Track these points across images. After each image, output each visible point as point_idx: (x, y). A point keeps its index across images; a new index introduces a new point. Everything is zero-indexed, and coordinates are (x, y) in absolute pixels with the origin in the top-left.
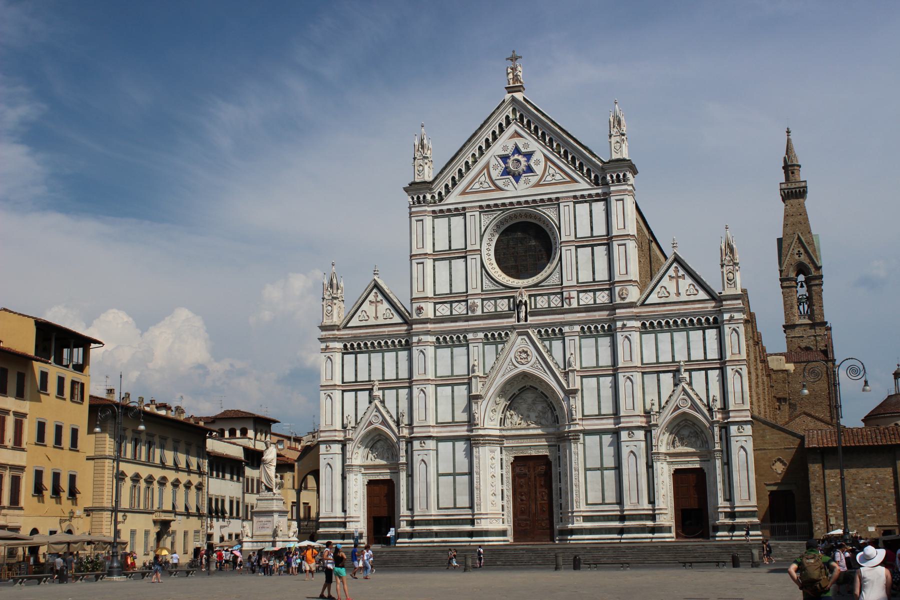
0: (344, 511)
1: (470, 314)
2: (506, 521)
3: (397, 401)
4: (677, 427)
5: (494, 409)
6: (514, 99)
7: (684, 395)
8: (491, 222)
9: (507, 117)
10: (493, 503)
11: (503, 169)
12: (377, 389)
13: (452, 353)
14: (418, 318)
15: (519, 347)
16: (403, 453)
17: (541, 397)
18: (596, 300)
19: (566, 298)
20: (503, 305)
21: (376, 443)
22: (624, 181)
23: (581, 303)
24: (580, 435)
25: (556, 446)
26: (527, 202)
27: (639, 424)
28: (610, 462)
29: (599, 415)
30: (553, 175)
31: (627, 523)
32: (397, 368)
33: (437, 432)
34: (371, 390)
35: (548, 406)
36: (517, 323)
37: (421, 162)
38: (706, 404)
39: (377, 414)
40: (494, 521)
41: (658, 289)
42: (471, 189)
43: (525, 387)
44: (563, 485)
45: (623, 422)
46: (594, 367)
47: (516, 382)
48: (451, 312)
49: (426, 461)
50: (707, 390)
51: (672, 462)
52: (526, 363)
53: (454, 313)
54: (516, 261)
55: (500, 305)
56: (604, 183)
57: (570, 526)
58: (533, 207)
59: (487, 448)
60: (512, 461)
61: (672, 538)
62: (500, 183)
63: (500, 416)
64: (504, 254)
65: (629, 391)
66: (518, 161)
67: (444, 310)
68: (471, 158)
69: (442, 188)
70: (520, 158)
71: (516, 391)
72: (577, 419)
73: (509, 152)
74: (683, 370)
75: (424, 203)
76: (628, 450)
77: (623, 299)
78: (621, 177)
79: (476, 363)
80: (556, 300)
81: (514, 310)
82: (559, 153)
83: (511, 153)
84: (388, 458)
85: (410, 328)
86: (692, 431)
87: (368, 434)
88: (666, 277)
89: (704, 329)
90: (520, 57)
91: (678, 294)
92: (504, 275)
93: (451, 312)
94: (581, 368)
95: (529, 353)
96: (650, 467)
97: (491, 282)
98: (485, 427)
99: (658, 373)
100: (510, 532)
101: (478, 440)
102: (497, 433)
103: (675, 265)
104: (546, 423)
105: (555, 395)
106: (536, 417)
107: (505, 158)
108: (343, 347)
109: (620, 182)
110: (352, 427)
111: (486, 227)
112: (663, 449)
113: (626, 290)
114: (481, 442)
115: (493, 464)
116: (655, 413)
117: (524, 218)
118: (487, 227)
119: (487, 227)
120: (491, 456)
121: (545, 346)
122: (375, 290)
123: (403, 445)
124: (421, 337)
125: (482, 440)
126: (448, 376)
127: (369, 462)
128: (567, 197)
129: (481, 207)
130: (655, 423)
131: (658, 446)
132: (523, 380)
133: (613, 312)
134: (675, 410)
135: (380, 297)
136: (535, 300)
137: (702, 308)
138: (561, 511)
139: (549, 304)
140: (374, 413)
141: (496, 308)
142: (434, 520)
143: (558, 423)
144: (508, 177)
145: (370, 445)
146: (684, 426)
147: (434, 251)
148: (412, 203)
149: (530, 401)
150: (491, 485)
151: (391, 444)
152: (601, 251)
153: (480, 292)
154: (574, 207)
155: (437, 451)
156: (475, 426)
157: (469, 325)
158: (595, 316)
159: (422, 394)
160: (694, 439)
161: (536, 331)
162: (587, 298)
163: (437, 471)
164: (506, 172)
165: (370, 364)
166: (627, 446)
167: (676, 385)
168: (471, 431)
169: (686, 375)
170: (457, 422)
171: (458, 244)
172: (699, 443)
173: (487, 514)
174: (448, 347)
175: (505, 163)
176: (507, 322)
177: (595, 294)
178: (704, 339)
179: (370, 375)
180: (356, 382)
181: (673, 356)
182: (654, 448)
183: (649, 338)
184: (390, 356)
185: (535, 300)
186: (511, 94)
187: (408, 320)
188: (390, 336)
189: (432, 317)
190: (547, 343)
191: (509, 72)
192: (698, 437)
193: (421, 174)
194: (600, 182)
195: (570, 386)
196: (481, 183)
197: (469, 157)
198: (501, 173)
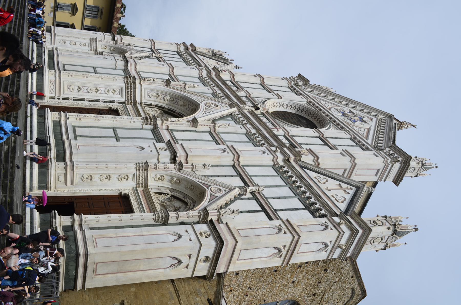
5: (159, 96)
7: (225, 191)
12: (157, 56)
24: (150, 124)
26: (331, 118)
59: (123, 85)
61: (31, 190)
63: (153, 103)
101: (130, 78)
102: (138, 100)
103: (354, 189)
114: (129, 81)
117: (317, 122)
120: (116, 90)
132: (190, 111)
134: (205, 184)
150: (88, 87)
166: (149, 146)
173: (60, 77)
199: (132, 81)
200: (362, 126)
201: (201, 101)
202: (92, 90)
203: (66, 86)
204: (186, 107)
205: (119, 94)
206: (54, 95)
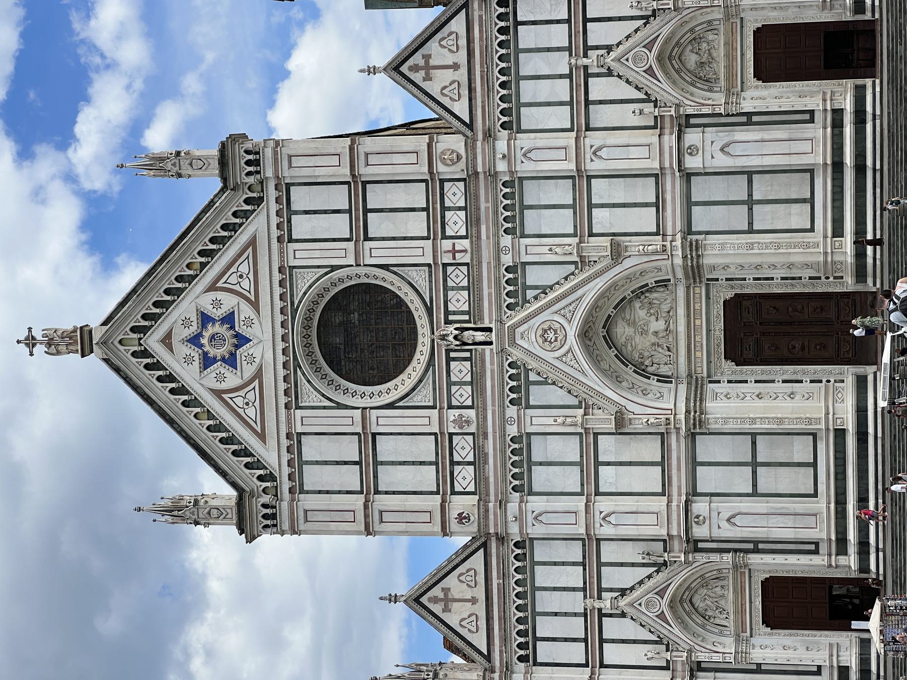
0: (818, 671)
1: (472, 429)
2: (840, 377)
3: (622, 565)
4: (682, 74)
5: (642, 391)
6: (104, 343)
7: (627, 60)
8: (315, 389)
9: (134, 354)
10: (807, 396)
11: (224, 365)
12: (601, 601)
13: (541, 464)
14: (476, 524)
15: (535, 344)
16: (715, 557)
17: (623, 309)
18: (460, 207)
19: (454, 258)
20: (461, 370)
21: (696, 609)
22: (258, 153)
23: (463, 232)
25: (707, 285)
26: (283, 325)
27: (674, 137)
28: (737, 189)
29: (656, 205)
30: (241, 276)
31: (848, 159)
32: (563, 564)
33: (680, 495)
34: (601, 615)
35: (640, 298)
36: (493, 347)
37: (203, 513)
38: (645, 21)
39: (643, 601)
40: (840, 395)
41: (445, 101)
42: (256, 422)
43: (604, 337)
44: (777, 274)
45: (671, 164)
46: (575, 213)
47: (596, 352)
48: (469, 463)
49: (732, 513)
50: (620, 19)
51: (742, 82)
52: (564, 332)
53: (470, 458)
54: (384, 348)
55: (461, 376)
56: (260, 189)
57: (850, 259)
58: (294, 313)
60: (734, 363)
61: (874, 82)
62: (249, 371)
63: (653, 381)
64: (373, 370)
65: (617, 153)
66: (212, 338)
67: (465, 477)
68: (202, 422)
69: (251, 474)
70: (207, 334)
71: (613, 353)
72: (664, 243)
73: (196, 354)
74: (585, 61)
75: (275, 507)
76: (719, 155)
77: (459, 158)
78: (251, 157)
79: (560, 420)
80: (457, 276)
81: (470, 351)
82: (203, 265)
83: (197, 349)
84: (722, 587)
85: (494, 539)
86: (690, 47)
87: (677, 617)
88: (425, 85)
89: (517, 23)
90: (30, 329)
91: (455, 67)
92: (409, 369)
93: (469, 463)
94: (575, 235)
95: (545, 326)
96: (749, 119)
97: (420, 391)
98: (672, 407)
99: (588, 103)
100: (860, 369)
101: (694, 419)
102: (683, 389)
103: (404, 69)
104: (668, 301)
105: (620, 284)
106: (657, 319)
107: (207, 361)
108: (523, 664)
109: (259, 160)
110: (667, 650)
111: (323, 399)
112: (720, 98)
113: (443, 153)
115: (738, 396)
116: (657, 109)
118: (323, 395)
119: (323, 395)
121: (536, 298)
122: (424, 600)
123: (701, 558)
124: (510, 518)
125: (695, 412)
126: (582, 471)
127: (731, 623)
128: (281, 252)
129: (287, 406)
130: (673, 109)
131: (713, 105)
133: (481, 177)
135: (437, 592)
136: (454, 313)
137: (481, 26)
138: (823, 278)
139: (463, 288)
140: (643, 609)
141: (465, 383)
142: (837, 503)
143: (669, 280)
144: (238, 357)
145: (699, 620)
146: (680, 61)
147: (361, 492)
148: (275, 529)
149: (629, 331)
151: (699, 580)
152: (376, 197)
153: (436, 411)
154: (297, 241)
155: (712, 495)
156: (669, 424)
157: (494, 432)
158: (487, 208)
159: (612, 519)
160: (705, 45)
161: (509, 312)
162: (455, 223)
163: (747, 495)
164: (231, 361)
165: (556, 614)
166: (713, 157)
167: (610, 73)
168: (678, 430)
169: (593, 54)
170: (663, 457)
171: (350, 449)
172: (711, 37)
174: (530, 470)
175: (214, 360)
176: (492, 364)
177: (449, 209)
178: (534, 23)
179: (575, 615)
180: (585, 640)
181: (561, 76)
182: (717, 111)
183: (530, 117)
184: (543, 576)
185: (454, 313)
186: (95, 347)
187: (478, 544)
188: (504, 576)
189: (477, 497)
190: (530, 294)
191: (55, 351)
192: (700, 38)
193: (225, 513)
194: (255, 195)
195: (606, 254)
196: (247, 404)
197: (200, 424)
198: (231, 369)
199: (692, 413)
200: (220, 295)
201: (570, 354)
202: (769, 397)
203: (815, 397)
204: (598, 352)
205: (718, 395)
206: (836, 384)
